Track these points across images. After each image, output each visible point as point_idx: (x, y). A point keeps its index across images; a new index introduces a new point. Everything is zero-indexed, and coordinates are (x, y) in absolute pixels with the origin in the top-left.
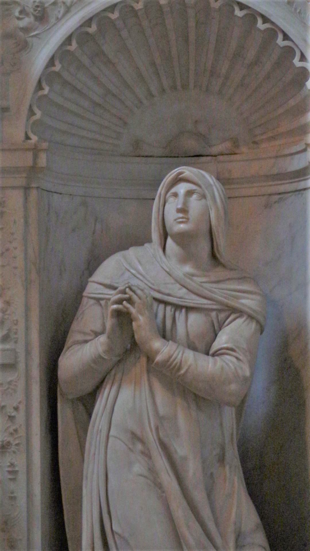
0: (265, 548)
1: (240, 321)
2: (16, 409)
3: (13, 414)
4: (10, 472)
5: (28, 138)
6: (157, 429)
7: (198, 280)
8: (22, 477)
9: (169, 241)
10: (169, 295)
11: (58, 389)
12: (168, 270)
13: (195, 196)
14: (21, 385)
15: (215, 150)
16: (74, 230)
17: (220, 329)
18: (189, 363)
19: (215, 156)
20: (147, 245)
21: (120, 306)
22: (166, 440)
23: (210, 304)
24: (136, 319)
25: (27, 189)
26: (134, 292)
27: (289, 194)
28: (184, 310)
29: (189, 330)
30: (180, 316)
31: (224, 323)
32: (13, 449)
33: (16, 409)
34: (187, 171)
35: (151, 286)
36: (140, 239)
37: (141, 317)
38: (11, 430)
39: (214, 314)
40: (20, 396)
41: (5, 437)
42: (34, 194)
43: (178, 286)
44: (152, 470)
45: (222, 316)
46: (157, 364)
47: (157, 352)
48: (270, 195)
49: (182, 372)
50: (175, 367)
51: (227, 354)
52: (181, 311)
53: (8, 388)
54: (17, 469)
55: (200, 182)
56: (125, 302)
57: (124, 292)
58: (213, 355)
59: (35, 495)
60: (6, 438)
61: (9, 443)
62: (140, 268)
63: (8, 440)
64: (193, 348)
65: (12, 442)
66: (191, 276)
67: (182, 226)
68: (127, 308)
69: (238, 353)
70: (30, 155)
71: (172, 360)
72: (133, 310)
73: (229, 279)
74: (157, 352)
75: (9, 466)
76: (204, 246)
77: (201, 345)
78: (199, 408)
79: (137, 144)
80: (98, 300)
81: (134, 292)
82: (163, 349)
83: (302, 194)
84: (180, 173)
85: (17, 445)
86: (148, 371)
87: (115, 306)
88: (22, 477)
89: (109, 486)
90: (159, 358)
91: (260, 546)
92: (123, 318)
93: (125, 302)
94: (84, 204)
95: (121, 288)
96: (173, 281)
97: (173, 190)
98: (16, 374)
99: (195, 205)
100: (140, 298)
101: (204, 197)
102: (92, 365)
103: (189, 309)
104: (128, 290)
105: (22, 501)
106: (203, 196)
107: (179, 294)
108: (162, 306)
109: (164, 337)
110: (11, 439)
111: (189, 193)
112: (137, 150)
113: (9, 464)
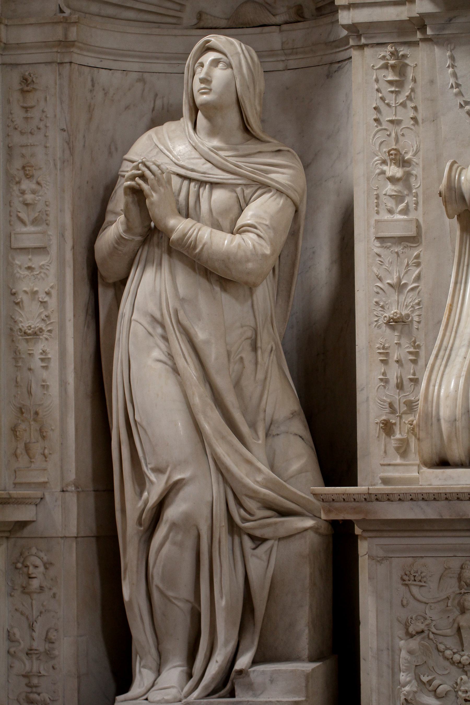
1: (267, 196)
2: (48, 294)
3: (45, 300)
4: (42, 360)
5: (61, 11)
6: (176, 312)
7: (222, 153)
8: (54, 365)
10: (193, 170)
11: (99, 273)
12: (194, 145)
13: (221, 65)
14: (53, 270)
16: (127, 108)
18: (204, 241)
19: (279, 25)
20: (182, 119)
21: (133, 183)
22: (185, 322)
23: (235, 179)
24: (152, 196)
27: (347, 62)
28: (207, 186)
29: (212, 207)
30: (204, 192)
31: (250, 199)
32: (44, 336)
33: (48, 294)
34: (215, 39)
35: (176, 161)
36: (175, 115)
37: (154, 194)
38: (43, 316)
39: (239, 190)
40: (52, 281)
41: (38, 323)
43: (203, 161)
44: (171, 356)
45: (248, 191)
46: (172, 241)
48: (331, 63)
49: (197, 250)
53: (40, 272)
54: (49, 356)
55: (226, 51)
56: (137, 179)
59: (69, 384)
60: (38, 325)
61: (41, 330)
63: (40, 326)
64: (217, 226)
65: (44, 328)
67: (205, 96)
68: (139, 185)
69: (259, 230)
72: (145, 186)
73: (260, 152)
75: (41, 354)
76: (233, 118)
77: (226, 224)
78: (224, 289)
79: (200, 15)
84: (208, 41)
85: (50, 331)
88: (54, 365)
90: (174, 236)
91: (296, 434)
93: (137, 179)
94: (142, 80)
96: (197, 155)
97: (200, 61)
98: (48, 258)
99: (220, 75)
101: (229, 66)
102: (116, 245)
103: (214, 185)
105: (55, 389)
106: (229, 66)
107: (203, 168)
108: (186, 182)
110: (43, 325)
111: (216, 63)
113: (41, 351)
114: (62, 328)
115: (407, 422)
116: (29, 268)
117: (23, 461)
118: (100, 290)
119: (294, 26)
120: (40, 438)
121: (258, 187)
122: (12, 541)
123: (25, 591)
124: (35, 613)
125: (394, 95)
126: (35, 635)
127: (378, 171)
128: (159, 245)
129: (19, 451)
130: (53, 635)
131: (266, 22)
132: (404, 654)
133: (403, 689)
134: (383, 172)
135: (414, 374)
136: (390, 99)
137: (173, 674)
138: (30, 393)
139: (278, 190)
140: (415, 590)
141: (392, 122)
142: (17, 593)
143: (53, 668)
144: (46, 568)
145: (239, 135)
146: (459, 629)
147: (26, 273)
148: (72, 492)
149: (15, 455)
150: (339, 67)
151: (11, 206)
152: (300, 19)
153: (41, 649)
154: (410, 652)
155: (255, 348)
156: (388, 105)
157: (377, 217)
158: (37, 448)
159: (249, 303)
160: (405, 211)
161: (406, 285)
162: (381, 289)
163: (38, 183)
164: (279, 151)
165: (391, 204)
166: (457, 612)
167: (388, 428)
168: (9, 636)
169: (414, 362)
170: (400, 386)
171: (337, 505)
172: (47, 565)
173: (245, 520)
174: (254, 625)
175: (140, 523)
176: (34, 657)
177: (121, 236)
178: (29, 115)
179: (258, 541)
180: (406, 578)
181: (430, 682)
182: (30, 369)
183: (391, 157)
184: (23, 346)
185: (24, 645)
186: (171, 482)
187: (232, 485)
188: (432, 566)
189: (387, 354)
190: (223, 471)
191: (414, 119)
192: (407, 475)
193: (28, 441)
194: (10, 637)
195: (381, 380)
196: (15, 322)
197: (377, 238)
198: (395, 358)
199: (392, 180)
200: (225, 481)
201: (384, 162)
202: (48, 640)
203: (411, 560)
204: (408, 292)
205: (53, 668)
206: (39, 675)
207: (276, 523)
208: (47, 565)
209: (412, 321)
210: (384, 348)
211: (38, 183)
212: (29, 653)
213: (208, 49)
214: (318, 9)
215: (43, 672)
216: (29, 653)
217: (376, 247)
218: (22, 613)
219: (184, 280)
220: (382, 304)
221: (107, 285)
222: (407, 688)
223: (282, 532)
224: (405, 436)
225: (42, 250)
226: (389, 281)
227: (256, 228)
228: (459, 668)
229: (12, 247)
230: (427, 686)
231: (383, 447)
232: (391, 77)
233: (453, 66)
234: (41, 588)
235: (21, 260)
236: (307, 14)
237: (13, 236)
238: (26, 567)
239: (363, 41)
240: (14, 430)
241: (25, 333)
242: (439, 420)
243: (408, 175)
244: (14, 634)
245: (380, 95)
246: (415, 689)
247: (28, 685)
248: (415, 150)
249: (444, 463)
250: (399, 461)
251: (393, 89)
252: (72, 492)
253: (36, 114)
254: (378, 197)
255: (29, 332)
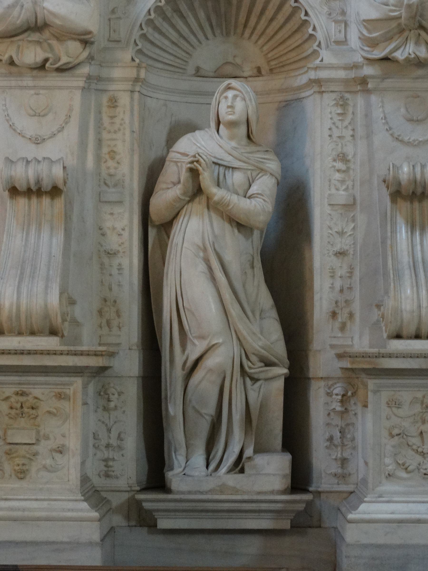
0: (277, 320)
5: (133, 60)
6: (214, 243)
9: (221, 126)
12: (221, 144)
13: (238, 99)
14: (127, 215)
15: (246, 74)
17: (253, 182)
19: (246, 78)
25: (132, 92)
26: (201, 156)
28: (231, 170)
30: (229, 174)
31: (255, 178)
33: (123, 230)
34: (234, 83)
35: (210, 154)
39: (249, 172)
40: (125, 222)
42: (136, 95)
43: (228, 155)
45: (254, 174)
47: (215, 194)
49: (230, 207)
50: (226, 203)
51: (257, 197)
52: (229, 170)
55: (242, 90)
56: (195, 163)
57: (195, 156)
58: (250, 198)
61: (118, 252)
62: (203, 143)
66: (235, 148)
68: (197, 167)
70: (135, 71)
71: (223, 200)
72: (200, 168)
74: (215, 194)
76: (243, 130)
77: (241, 192)
78: (239, 231)
79: (198, 69)
80: (176, 162)
81: (201, 156)
82: (218, 194)
83: (302, 101)
84: (229, 84)
85: (124, 252)
86: (208, 208)
87: (189, 165)
89: (182, 278)
91: (274, 318)
92: (194, 173)
93: (195, 163)
95: (192, 154)
96: (223, 151)
97: (225, 95)
100: (205, 161)
104: (197, 155)
108: (217, 167)
109: (218, 185)
111: (235, 97)
112: (198, 73)
114: (131, 251)
115: (345, 312)
116: (112, 214)
117: (106, 330)
118: (150, 229)
119: (257, 79)
120: (117, 317)
121: (258, 171)
122: (97, 378)
123: (106, 409)
124: (112, 423)
125: (341, 122)
126: (112, 435)
127: (330, 166)
128: (199, 203)
129: (103, 325)
130: (122, 436)
131: (238, 75)
132: (388, 447)
133: (387, 468)
134: (334, 167)
135: (350, 285)
136: (339, 124)
137: (199, 459)
138: (110, 289)
139: (271, 174)
140: (394, 409)
141: (339, 137)
142: (100, 410)
143: (123, 455)
144: (119, 395)
145: (245, 140)
146: (421, 433)
147: (109, 216)
148: (135, 350)
149: (101, 327)
150: (287, 105)
151: (100, 176)
152: (259, 75)
153: (115, 444)
154: (394, 447)
155: (253, 267)
156: (337, 127)
157: (329, 192)
158: (115, 323)
159: (250, 240)
160: (346, 189)
161: (346, 232)
162: (331, 234)
163: (118, 163)
164: (267, 151)
165: (339, 185)
166: (420, 424)
167: (334, 315)
168: (94, 436)
169: (350, 277)
170: (341, 291)
171: (358, 359)
172: (120, 394)
173: (250, 368)
174: (252, 431)
175: (183, 369)
176: (110, 449)
177: (179, 198)
178: (113, 121)
179: (255, 380)
180: (389, 403)
181: (403, 465)
182: (111, 275)
183: (340, 158)
184: (106, 260)
185: (104, 442)
186: (211, 345)
187: (245, 347)
188: (406, 396)
189: (334, 272)
190: (241, 338)
191: (353, 136)
192: (345, 343)
193: (108, 318)
194: (95, 436)
195: (330, 287)
196: (102, 246)
197: (330, 205)
198: (339, 275)
199: (338, 171)
200: (241, 344)
201: (335, 160)
202: (119, 438)
203: (393, 393)
204: (348, 237)
205: (123, 455)
206: (113, 460)
207: (267, 371)
208: (120, 394)
209: (349, 254)
210: (332, 269)
211: (118, 163)
212: (108, 446)
213: (229, 88)
214: (271, 70)
215: (115, 458)
216: (108, 446)
217: (328, 210)
218: (103, 422)
219: (219, 226)
220: (332, 243)
221: (154, 226)
222: (390, 467)
223: (270, 375)
224: (344, 320)
225: (120, 202)
226: (336, 230)
227: (263, 196)
228: (420, 455)
229: (101, 201)
230: (402, 466)
231: (331, 327)
232: (340, 111)
233: (383, 107)
234: (116, 406)
235: (107, 208)
236: (263, 72)
237: (101, 194)
238: (106, 394)
239: (323, 89)
240: (100, 312)
241: (108, 253)
242: (402, 311)
243: (348, 168)
244: (98, 435)
245: (333, 122)
246: (394, 468)
247: (106, 466)
248: (353, 153)
249: (398, 337)
250: (340, 335)
251: (341, 118)
252: (135, 350)
253: (117, 121)
254: (330, 181)
255: (111, 252)
